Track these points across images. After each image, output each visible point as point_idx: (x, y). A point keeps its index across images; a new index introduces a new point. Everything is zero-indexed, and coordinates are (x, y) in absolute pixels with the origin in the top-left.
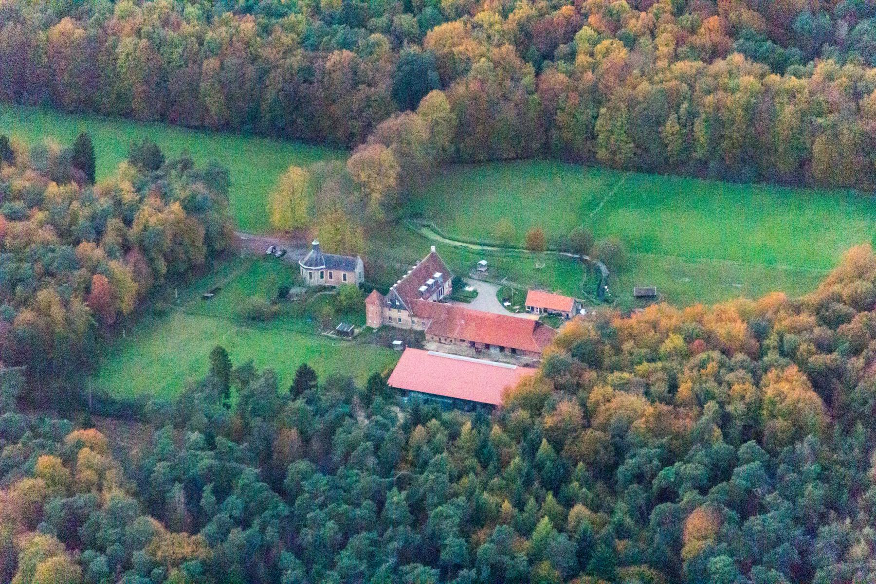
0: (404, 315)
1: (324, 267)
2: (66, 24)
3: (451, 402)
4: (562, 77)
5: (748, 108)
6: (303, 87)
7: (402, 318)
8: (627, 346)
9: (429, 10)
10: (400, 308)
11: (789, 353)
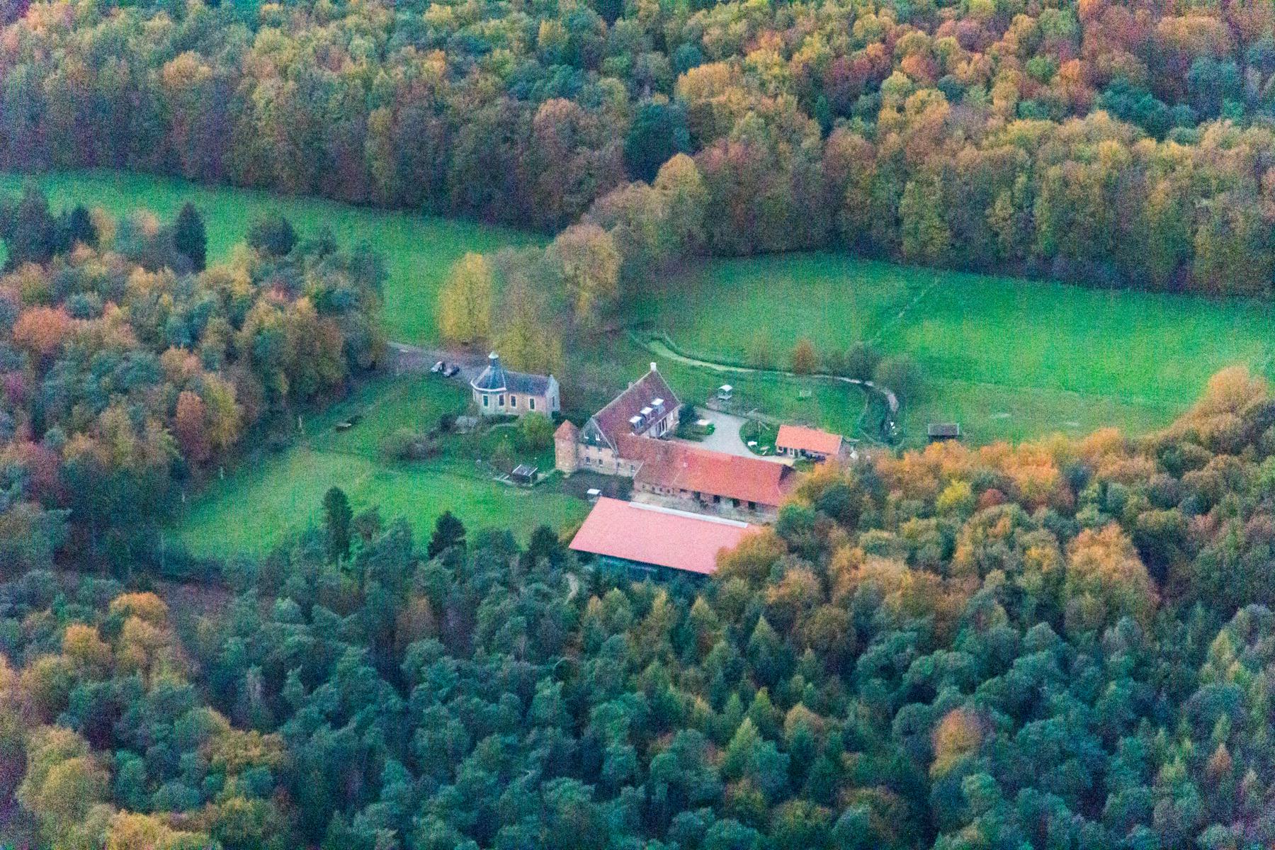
0: (606, 455)
1: (504, 389)
2: (187, 60)
4: (857, 139)
5: (1108, 185)
6: (503, 148)
7: (604, 459)
8: (893, 497)
9: (686, 48)
10: (601, 445)
11: (1113, 510)
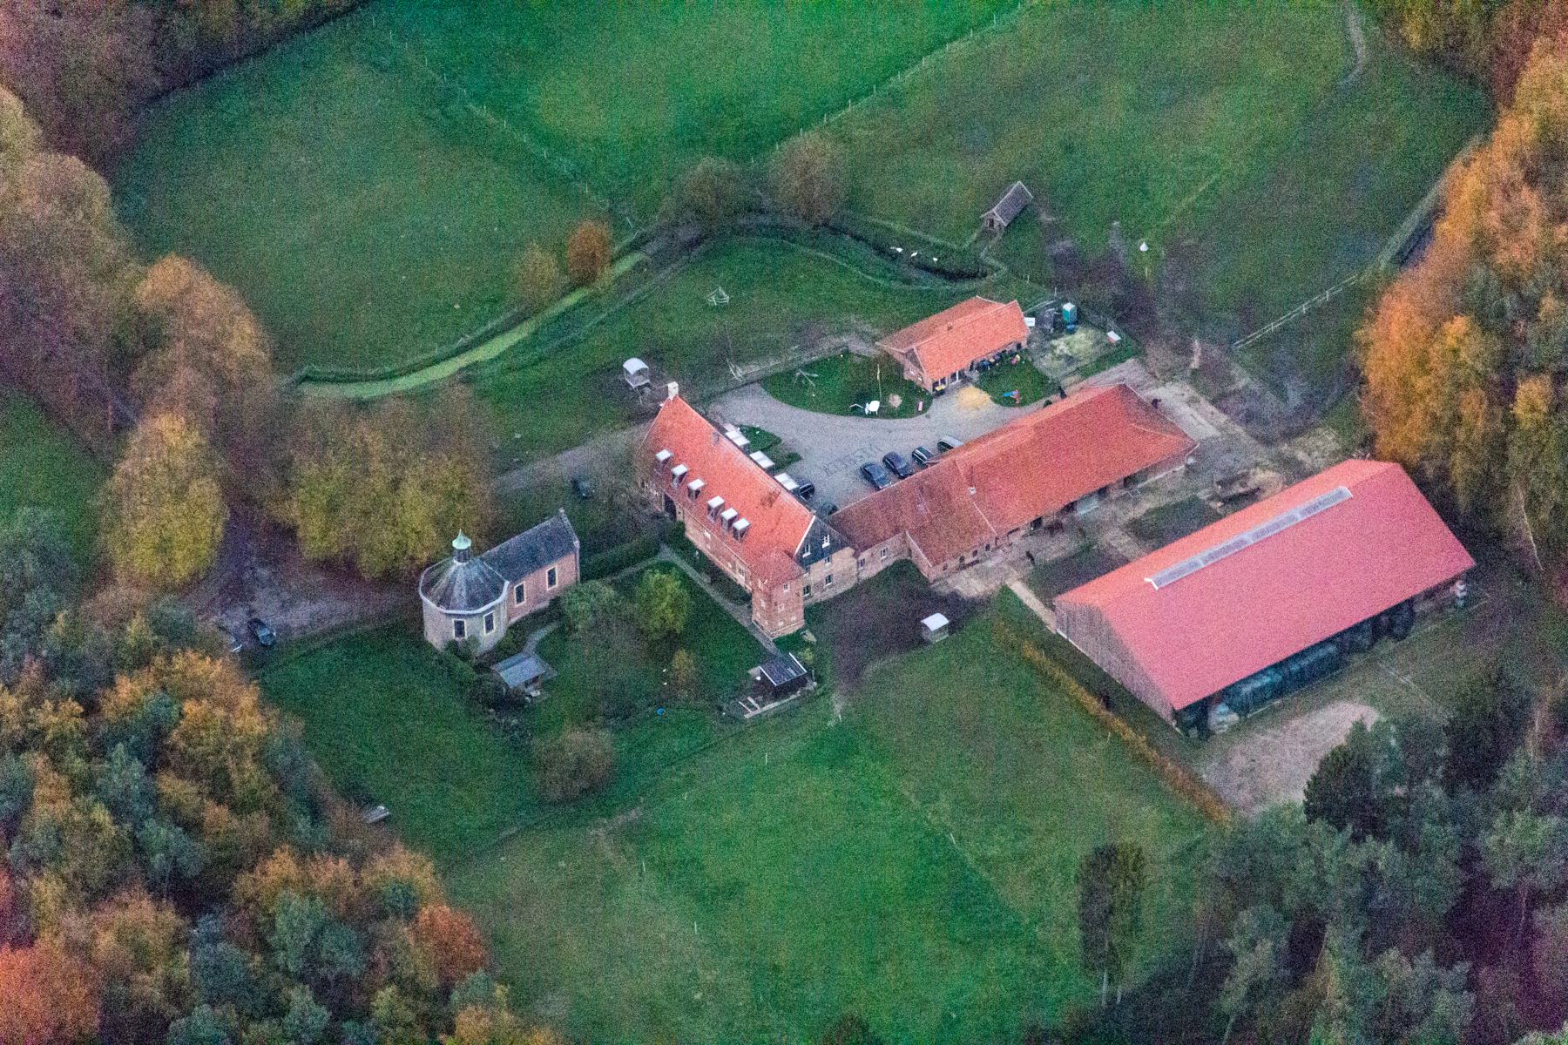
0: (842, 561)
3: (1331, 649)
10: (836, 546)
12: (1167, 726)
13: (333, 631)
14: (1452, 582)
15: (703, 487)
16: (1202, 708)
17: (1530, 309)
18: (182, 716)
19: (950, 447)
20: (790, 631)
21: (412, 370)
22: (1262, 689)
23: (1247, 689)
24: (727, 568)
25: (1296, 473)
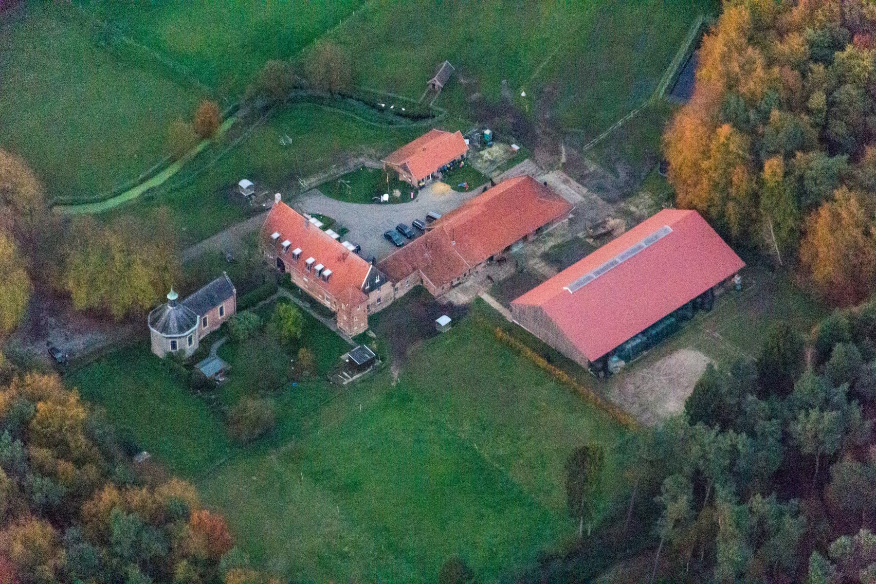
3: (673, 320)
10: (383, 282)
12: (585, 372)
13: (99, 351)
14: (733, 276)
15: (301, 253)
16: (604, 360)
17: (765, 118)
18: (37, 411)
19: (435, 219)
20: (361, 331)
21: (115, 195)
22: (637, 346)
23: (629, 346)
24: (319, 298)
25: (634, 221)
